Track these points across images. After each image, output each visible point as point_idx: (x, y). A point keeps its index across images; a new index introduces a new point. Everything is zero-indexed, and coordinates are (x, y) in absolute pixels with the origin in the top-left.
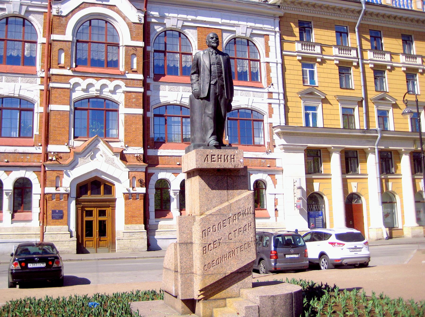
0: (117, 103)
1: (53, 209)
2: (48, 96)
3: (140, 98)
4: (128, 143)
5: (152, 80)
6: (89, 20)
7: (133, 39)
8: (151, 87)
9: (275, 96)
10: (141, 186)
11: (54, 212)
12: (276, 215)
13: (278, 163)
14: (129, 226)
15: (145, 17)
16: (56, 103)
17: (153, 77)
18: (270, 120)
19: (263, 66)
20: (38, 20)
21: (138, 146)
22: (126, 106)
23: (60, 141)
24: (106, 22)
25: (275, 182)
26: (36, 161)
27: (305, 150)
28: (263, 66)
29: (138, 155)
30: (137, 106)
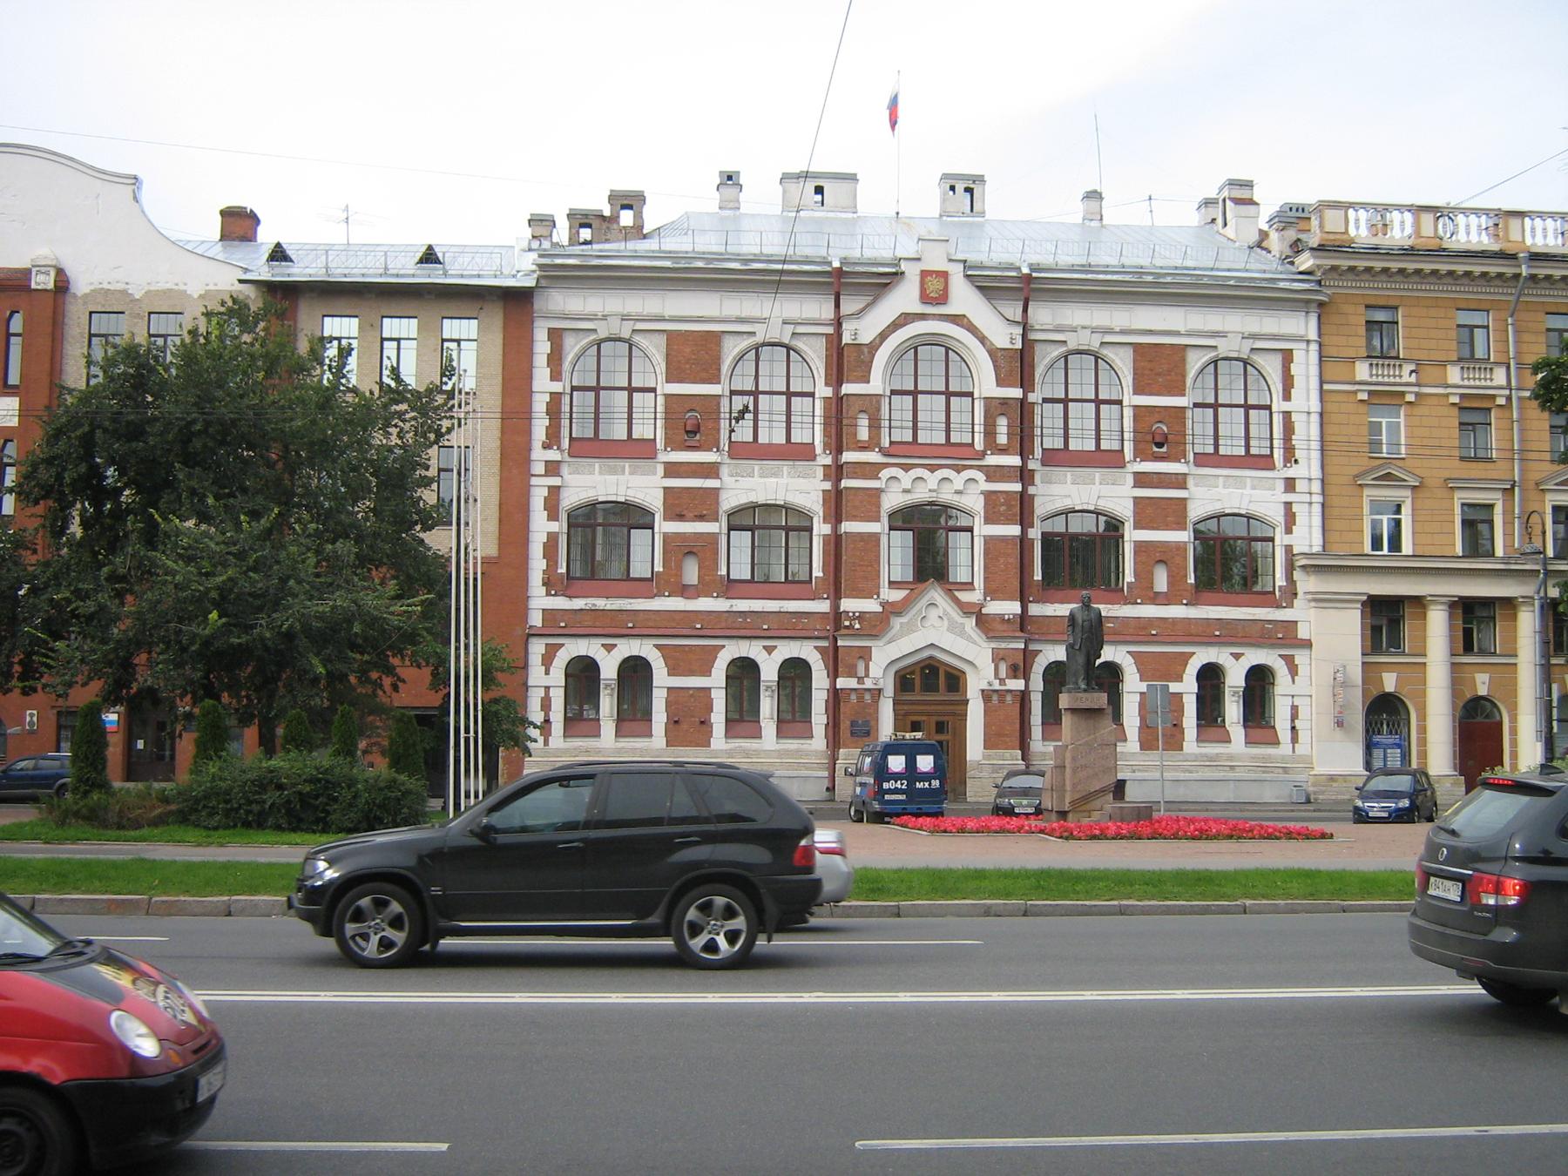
2: (837, 505)
4: (992, 592)
6: (914, 347)
7: (1000, 382)
9: (1300, 486)
10: (1015, 677)
11: (853, 723)
12: (1295, 740)
13: (1302, 633)
15: (1024, 336)
16: (854, 518)
18: (1287, 540)
19: (1278, 421)
21: (1012, 599)
24: (947, 349)
25: (1293, 670)
27: (1364, 604)
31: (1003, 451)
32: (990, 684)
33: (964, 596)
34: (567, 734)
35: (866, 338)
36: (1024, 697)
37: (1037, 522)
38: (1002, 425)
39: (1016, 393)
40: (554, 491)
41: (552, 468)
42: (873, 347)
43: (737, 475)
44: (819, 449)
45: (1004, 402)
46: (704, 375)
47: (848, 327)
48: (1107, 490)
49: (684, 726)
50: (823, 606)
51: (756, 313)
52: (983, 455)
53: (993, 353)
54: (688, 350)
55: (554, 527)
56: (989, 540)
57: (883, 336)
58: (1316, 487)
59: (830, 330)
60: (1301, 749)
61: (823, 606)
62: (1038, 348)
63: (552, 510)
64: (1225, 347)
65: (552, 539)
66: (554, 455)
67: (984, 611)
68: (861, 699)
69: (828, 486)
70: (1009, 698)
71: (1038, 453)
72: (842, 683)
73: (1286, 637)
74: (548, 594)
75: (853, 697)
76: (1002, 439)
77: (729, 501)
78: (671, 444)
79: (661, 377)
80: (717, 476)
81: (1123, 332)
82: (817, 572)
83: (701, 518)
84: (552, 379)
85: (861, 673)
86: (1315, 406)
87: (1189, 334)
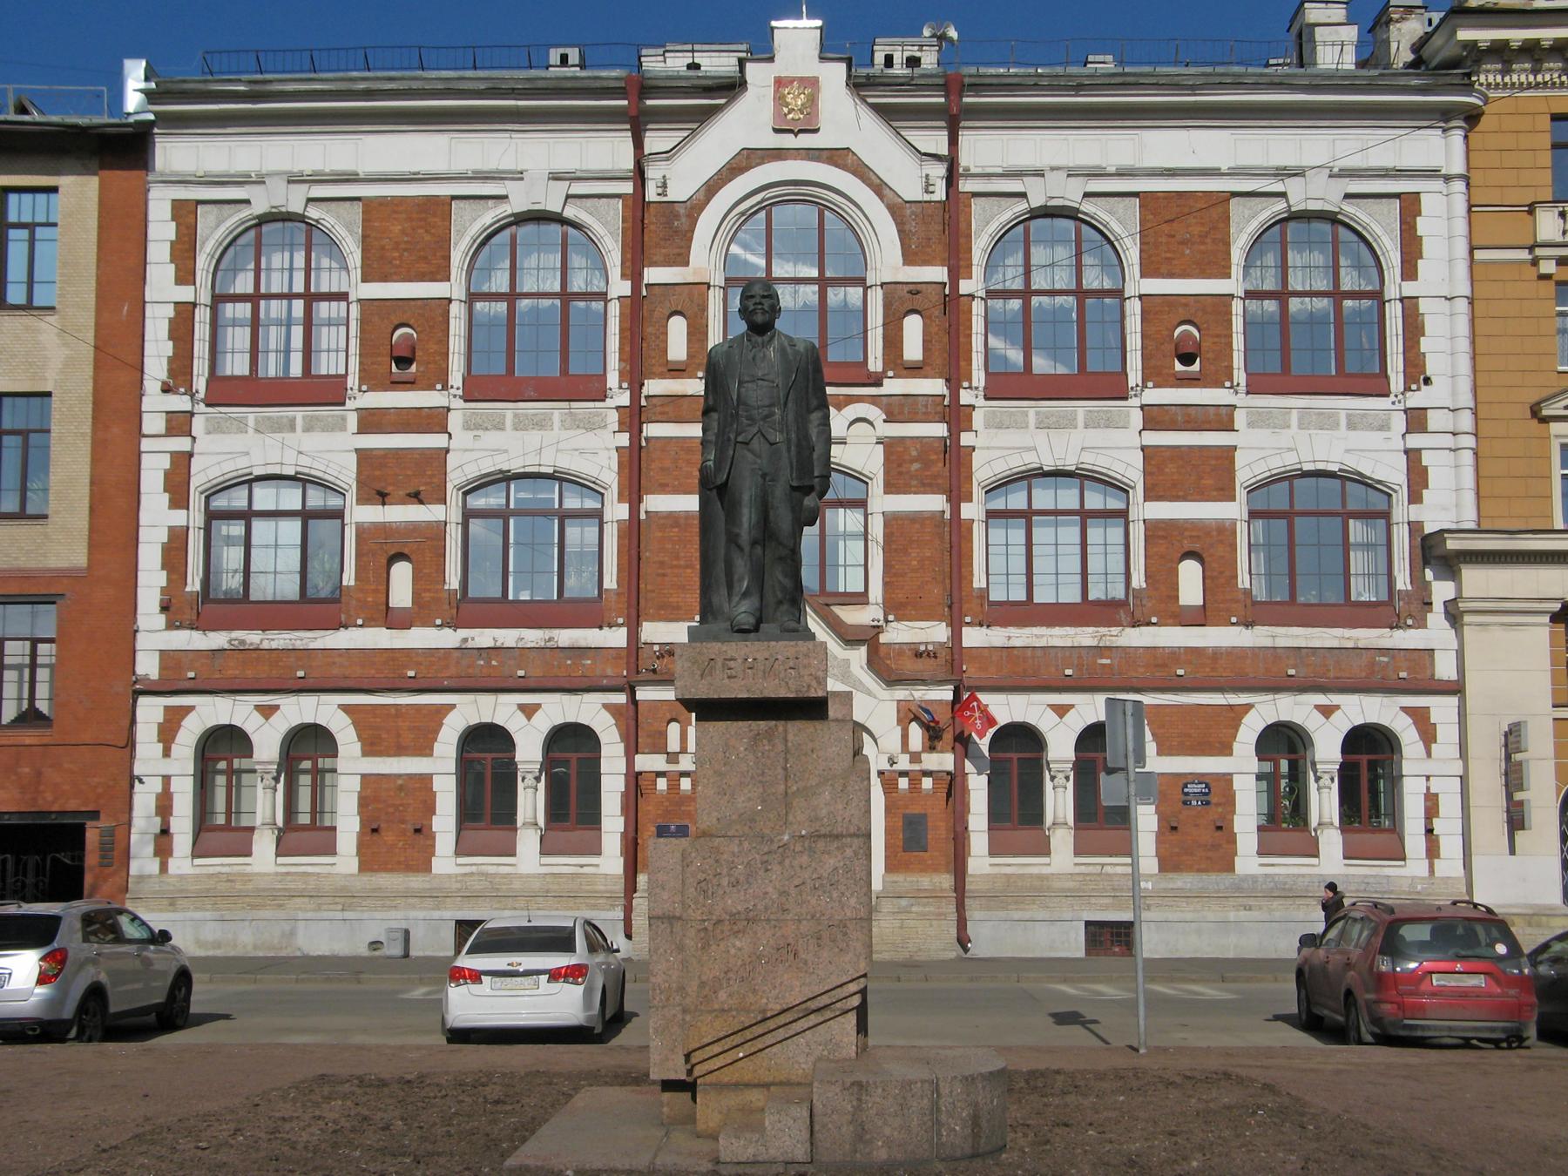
0: (862, 479)
1: (660, 821)
3: (934, 457)
4: (897, 607)
5: (981, 397)
7: (910, 258)
8: (978, 418)
9: (1435, 420)
12: (1433, 851)
13: (1445, 669)
14: (899, 878)
16: (664, 489)
17: (982, 384)
18: (1415, 513)
19: (1394, 312)
20: (605, 224)
22: (890, 488)
23: (678, 608)
24: (822, 208)
25: (1428, 734)
26: (609, 672)
28: (1394, 312)
29: (930, 648)
30: (924, 485)
31: (914, 370)
32: (892, 762)
33: (853, 616)
34: (198, 851)
35: (680, 191)
36: (953, 786)
37: (978, 493)
38: (913, 328)
39: (938, 273)
40: (182, 462)
41: (179, 424)
43: (478, 427)
44: (613, 379)
45: (915, 289)
46: (423, 267)
47: (653, 173)
48: (1096, 437)
49: (388, 836)
50: (616, 637)
51: (507, 164)
52: (877, 381)
53: (897, 209)
54: (397, 228)
55: (178, 518)
56: (893, 522)
57: (712, 188)
58: (1466, 421)
59: (627, 188)
60: (1450, 864)
61: (616, 637)
62: (977, 205)
63: (177, 488)
64: (1301, 195)
66: (180, 403)
67: (883, 638)
68: (674, 786)
69: (624, 439)
70: (927, 783)
71: (979, 377)
72: (645, 762)
73: (1412, 677)
74: (170, 626)
75: (662, 784)
76: (913, 349)
77: (460, 470)
78: (371, 380)
79: (357, 274)
80: (443, 429)
81: (1121, 174)
82: (610, 582)
83: (416, 498)
84: (180, 280)
85: (673, 744)
87: (1235, 173)
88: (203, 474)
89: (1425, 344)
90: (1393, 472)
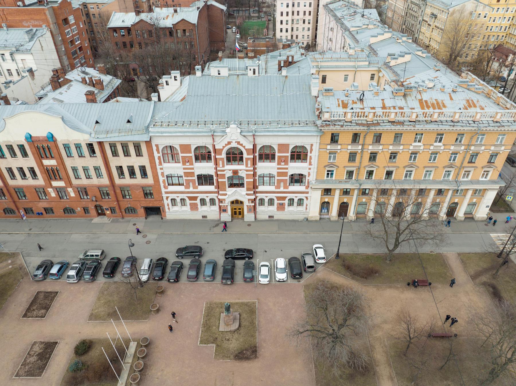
18: (308, 178)
42: (222, 149)
55: (164, 178)
65: (164, 181)
83: (192, 177)
86: (317, 154)
88: (165, 174)
89: (312, 161)
90: (307, 175)
